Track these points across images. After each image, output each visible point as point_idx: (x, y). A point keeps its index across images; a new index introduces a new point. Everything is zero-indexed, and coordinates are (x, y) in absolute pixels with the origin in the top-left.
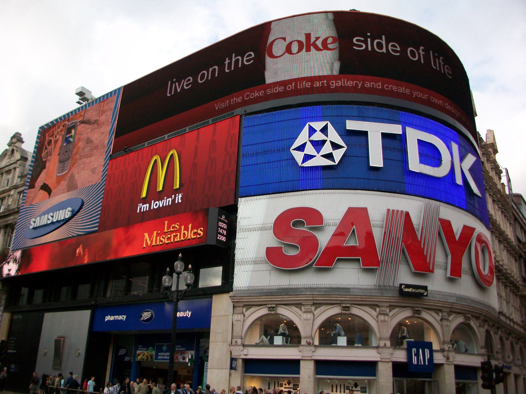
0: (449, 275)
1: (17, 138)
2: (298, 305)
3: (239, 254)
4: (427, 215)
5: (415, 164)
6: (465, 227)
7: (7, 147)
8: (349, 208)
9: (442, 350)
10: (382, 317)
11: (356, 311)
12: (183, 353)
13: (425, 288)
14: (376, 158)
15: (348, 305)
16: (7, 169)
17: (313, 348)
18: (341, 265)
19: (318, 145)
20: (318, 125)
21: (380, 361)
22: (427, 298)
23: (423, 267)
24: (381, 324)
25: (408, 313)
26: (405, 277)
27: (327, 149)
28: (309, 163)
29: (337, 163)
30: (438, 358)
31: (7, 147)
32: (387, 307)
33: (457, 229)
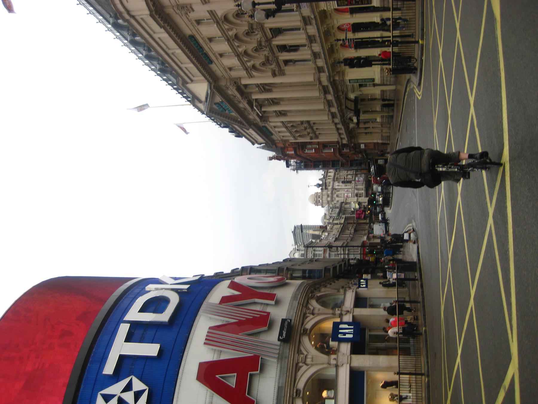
0: (273, 302)
4: (214, 311)
6: (229, 287)
9: (341, 315)
10: (309, 361)
11: (301, 385)
13: (283, 321)
14: (151, 349)
15: (295, 391)
18: (254, 392)
21: (350, 364)
22: (293, 321)
23: (263, 321)
25: (306, 340)
30: (348, 318)
32: (298, 355)
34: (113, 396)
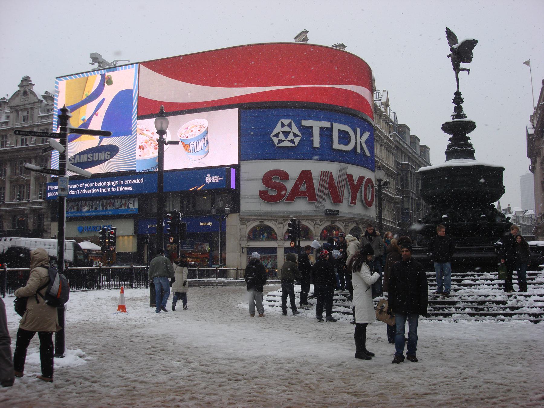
0: (350, 203)
1: (26, 82)
2: (276, 221)
3: (243, 193)
5: (336, 145)
7: (18, 89)
8: (303, 171)
12: (201, 244)
13: (338, 211)
14: (317, 143)
16: (22, 107)
17: (283, 242)
18: (298, 200)
19: (286, 134)
20: (286, 122)
24: (317, 230)
26: (328, 205)
27: (291, 137)
28: (281, 145)
29: (296, 144)
31: (18, 89)
33: (356, 178)
34: (291, 129)
